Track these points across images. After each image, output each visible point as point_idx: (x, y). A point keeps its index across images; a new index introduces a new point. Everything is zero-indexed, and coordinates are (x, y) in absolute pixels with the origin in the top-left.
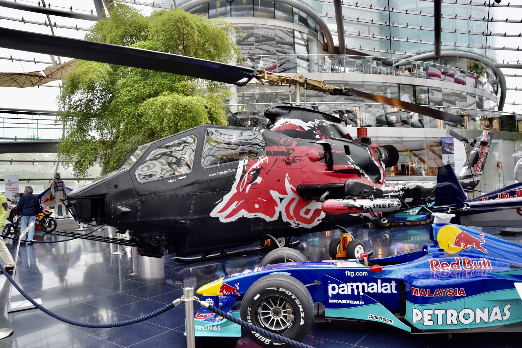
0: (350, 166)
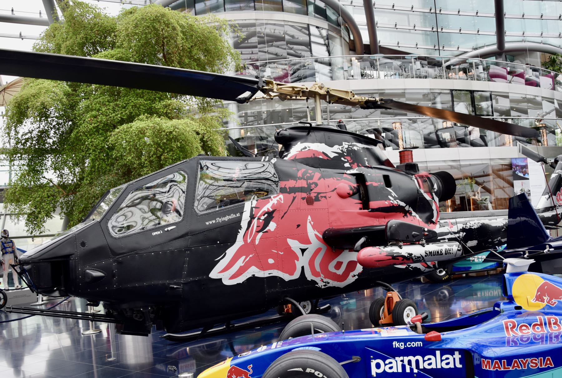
0: (391, 201)
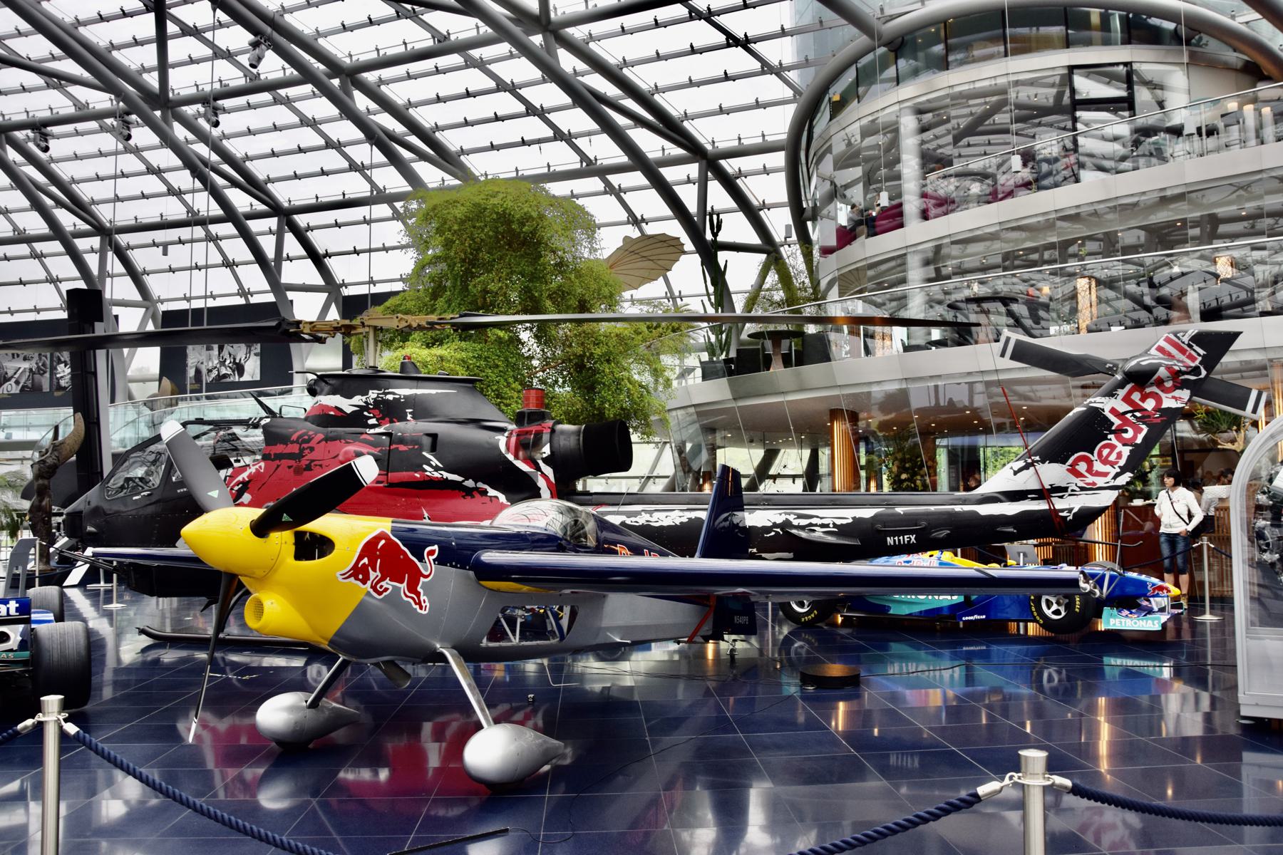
0: (428, 473)
